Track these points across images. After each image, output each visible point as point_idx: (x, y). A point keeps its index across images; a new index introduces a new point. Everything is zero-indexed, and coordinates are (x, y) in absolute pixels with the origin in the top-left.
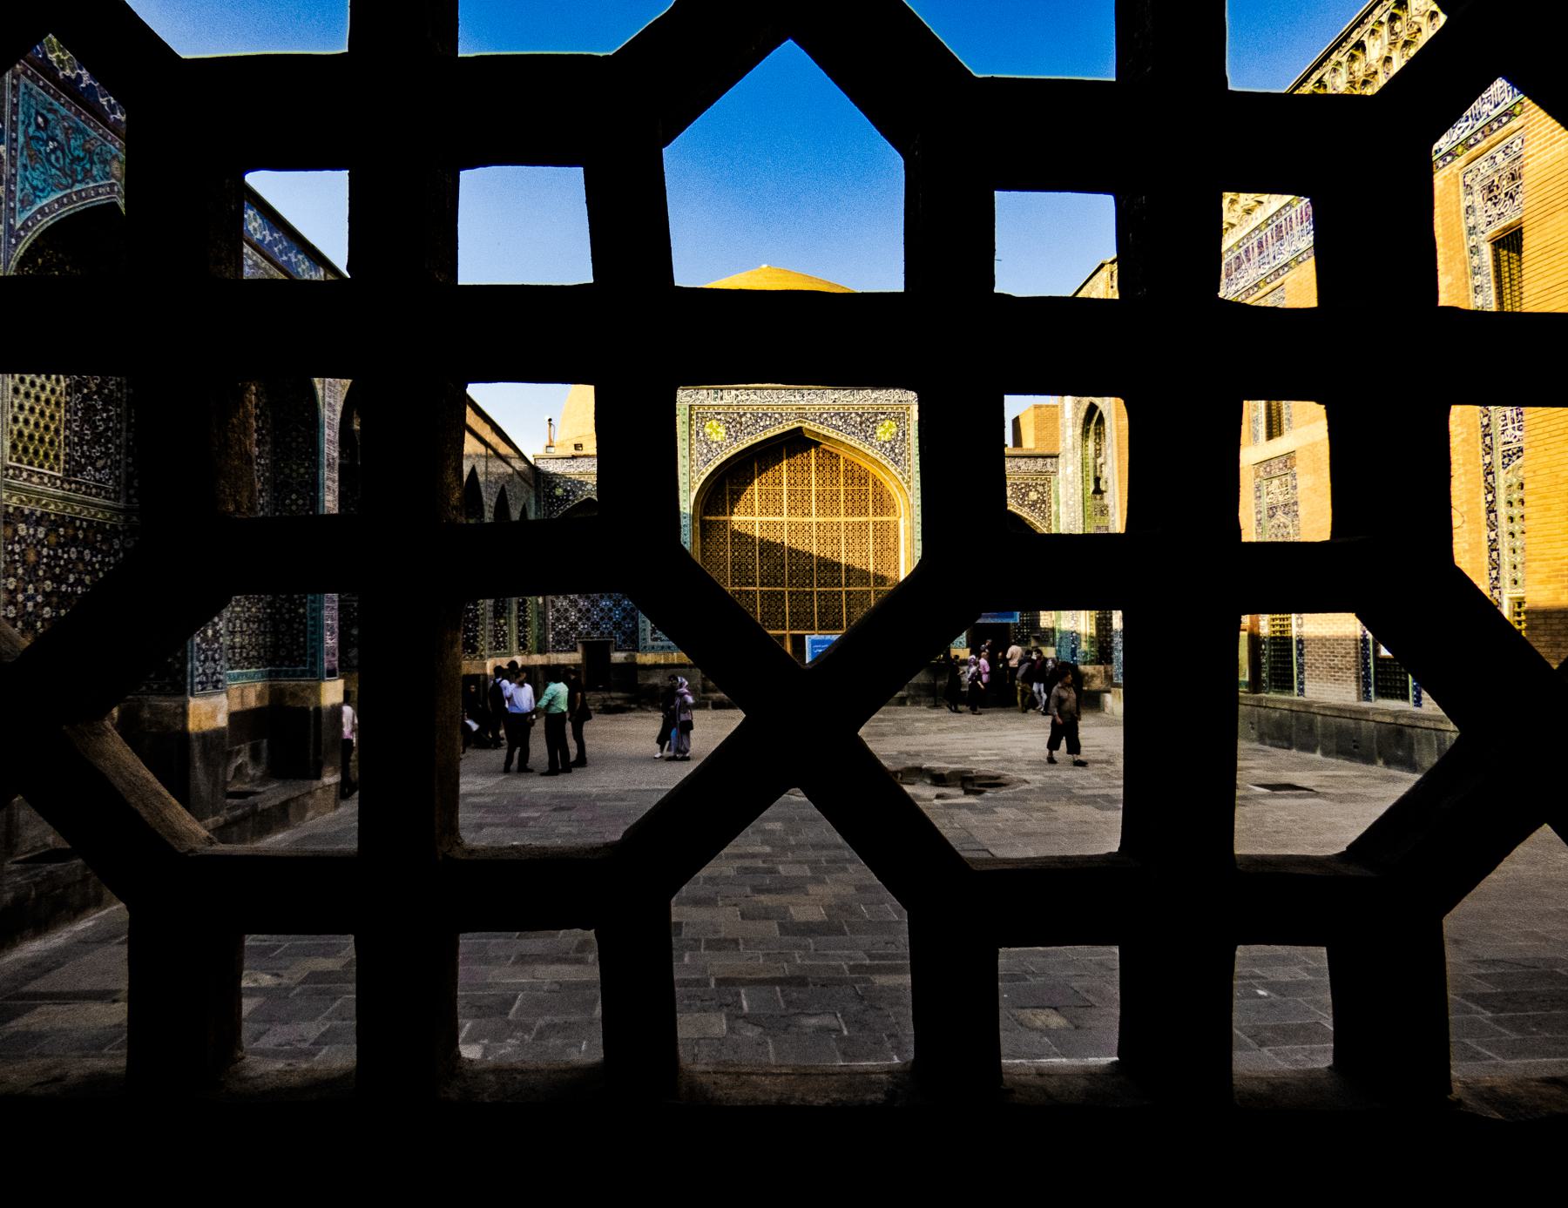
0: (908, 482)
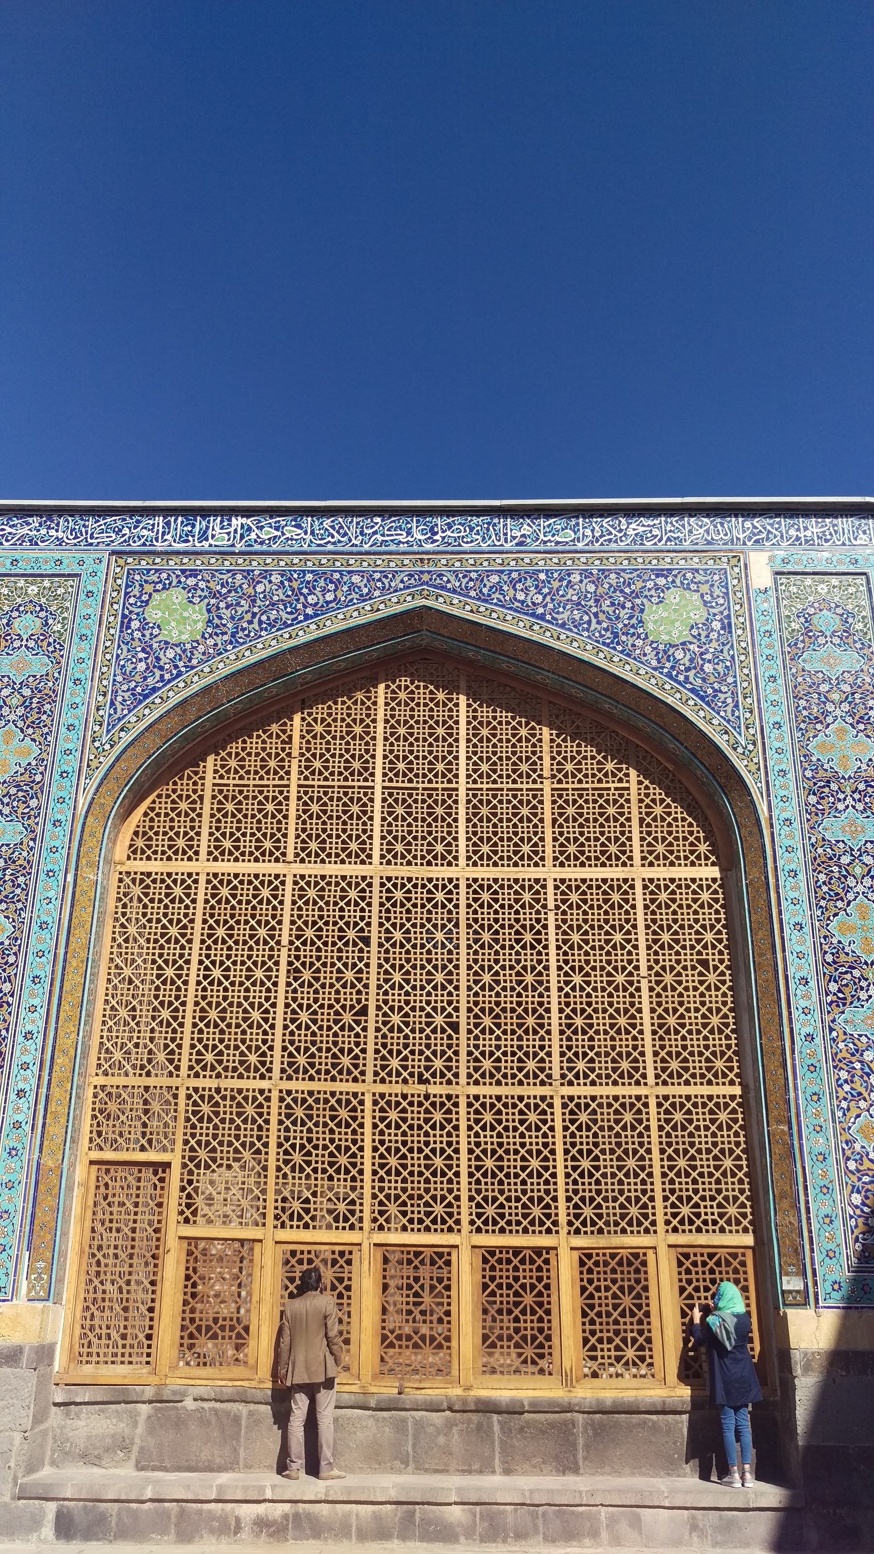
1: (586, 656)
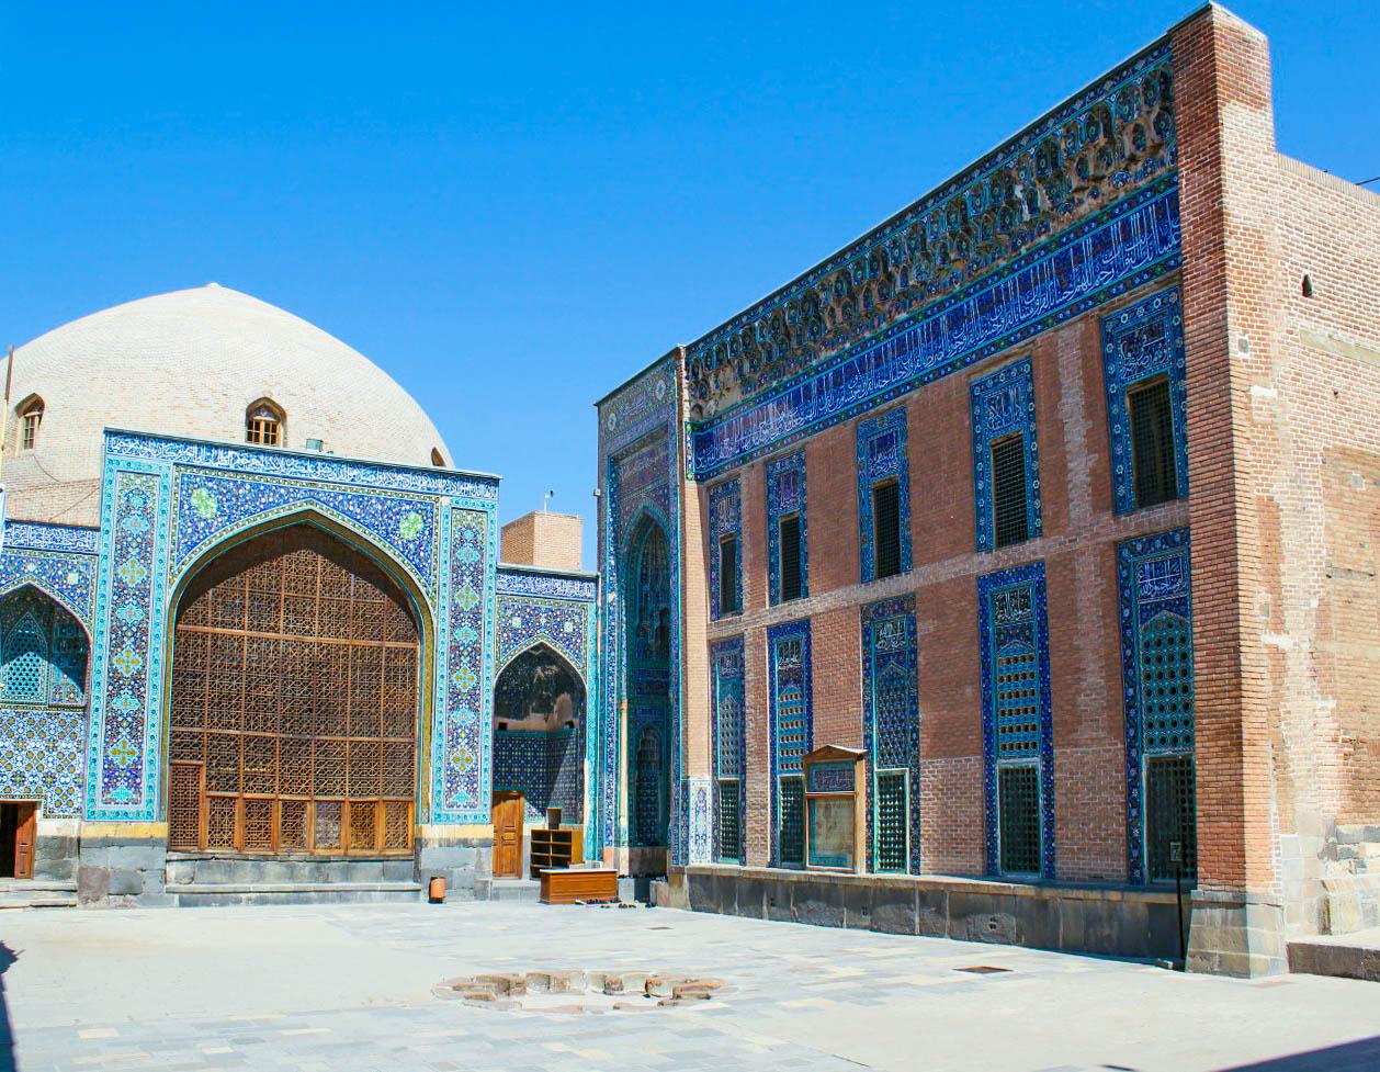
0: (432, 599)
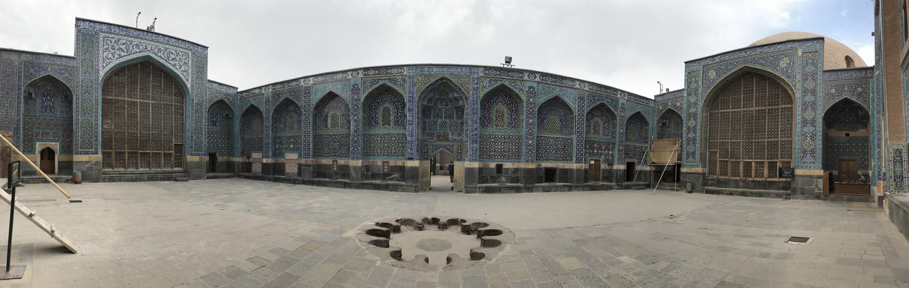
0: (794, 86)
1: (771, 71)
